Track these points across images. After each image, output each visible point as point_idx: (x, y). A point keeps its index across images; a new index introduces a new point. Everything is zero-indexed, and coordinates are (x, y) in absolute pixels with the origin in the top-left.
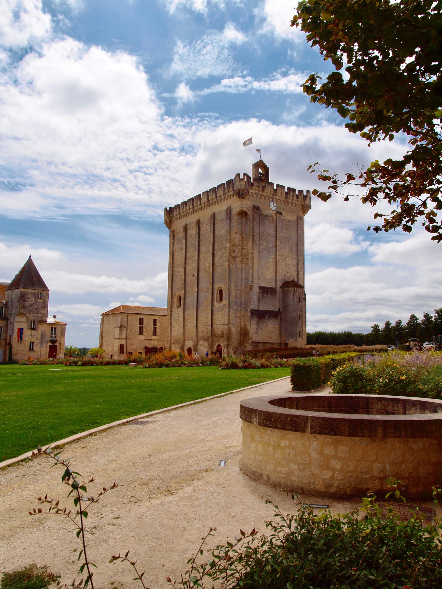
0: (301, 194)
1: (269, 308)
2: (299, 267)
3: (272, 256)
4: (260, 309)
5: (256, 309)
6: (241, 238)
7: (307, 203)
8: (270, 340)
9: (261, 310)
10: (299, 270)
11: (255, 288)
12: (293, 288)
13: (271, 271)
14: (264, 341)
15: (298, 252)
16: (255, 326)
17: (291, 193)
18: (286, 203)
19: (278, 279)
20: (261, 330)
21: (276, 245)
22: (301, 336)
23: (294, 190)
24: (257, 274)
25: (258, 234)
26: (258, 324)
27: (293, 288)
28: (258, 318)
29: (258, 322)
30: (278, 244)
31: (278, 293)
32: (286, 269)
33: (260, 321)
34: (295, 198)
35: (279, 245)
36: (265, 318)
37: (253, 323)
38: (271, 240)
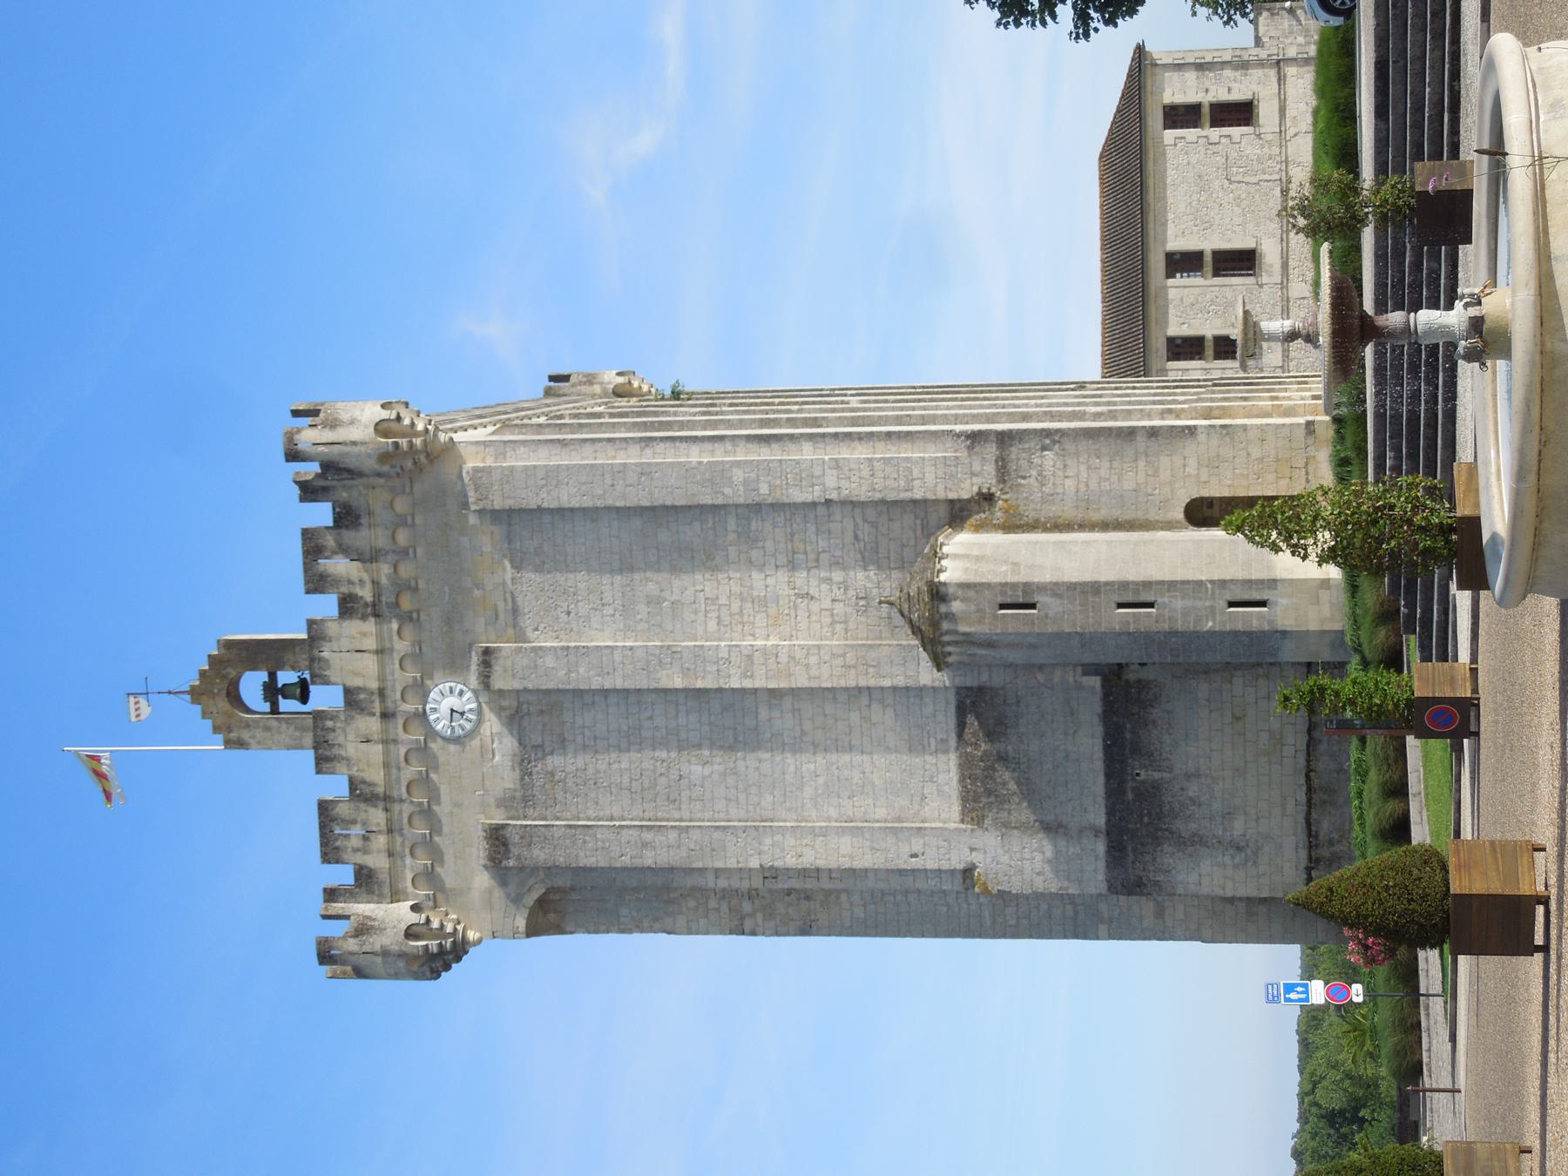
0: (325, 489)
1: (1090, 744)
2: (799, 496)
3: (764, 713)
4: (1098, 816)
5: (1101, 847)
6: (692, 903)
7: (371, 464)
8: (1288, 751)
9: (1110, 812)
10: (815, 494)
11: (976, 858)
12: (949, 649)
13: (855, 717)
14: (1302, 796)
15: (702, 508)
16: (1206, 866)
17: (338, 566)
18: (406, 603)
19: (900, 681)
20: (1228, 815)
21: (686, 691)
22: (1257, 596)
23: (312, 546)
24: (891, 840)
25: (648, 836)
26: (1197, 840)
27: (949, 649)
28: (1157, 841)
29: (1182, 842)
30: (678, 683)
31: (985, 677)
32: (827, 604)
33: (1178, 825)
34: (360, 538)
35: (686, 672)
36: (1156, 787)
37: (1193, 878)
38: (658, 722)
